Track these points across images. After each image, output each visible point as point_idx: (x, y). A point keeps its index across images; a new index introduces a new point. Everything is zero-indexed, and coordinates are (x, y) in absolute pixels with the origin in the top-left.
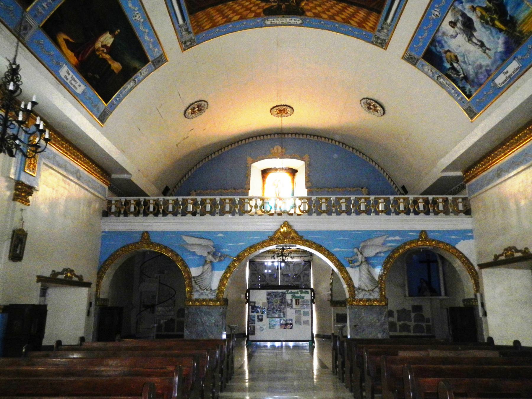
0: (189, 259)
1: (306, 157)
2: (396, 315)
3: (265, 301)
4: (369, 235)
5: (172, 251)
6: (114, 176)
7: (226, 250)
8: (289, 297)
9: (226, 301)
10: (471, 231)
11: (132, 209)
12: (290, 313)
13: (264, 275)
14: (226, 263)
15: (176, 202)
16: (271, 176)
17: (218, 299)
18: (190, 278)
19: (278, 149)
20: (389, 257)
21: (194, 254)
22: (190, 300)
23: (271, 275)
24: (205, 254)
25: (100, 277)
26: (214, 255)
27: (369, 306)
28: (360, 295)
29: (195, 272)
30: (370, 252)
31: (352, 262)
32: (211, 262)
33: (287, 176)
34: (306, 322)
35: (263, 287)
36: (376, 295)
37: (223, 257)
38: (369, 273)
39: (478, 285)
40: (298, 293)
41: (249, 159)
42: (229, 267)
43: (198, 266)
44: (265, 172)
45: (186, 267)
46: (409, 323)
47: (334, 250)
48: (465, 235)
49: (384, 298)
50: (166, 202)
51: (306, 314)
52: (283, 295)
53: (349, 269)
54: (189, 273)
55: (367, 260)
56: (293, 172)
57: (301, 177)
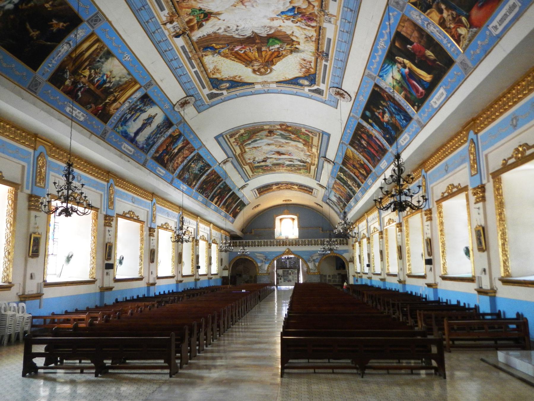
0: (258, 261)
1: (298, 214)
2: (331, 277)
3: (282, 273)
4: (315, 252)
5: (252, 258)
6: (232, 233)
7: (269, 258)
8: (290, 271)
9: (269, 273)
10: (348, 250)
11: (238, 244)
12: (290, 277)
13: (282, 262)
14: (269, 262)
15: (252, 242)
16: (283, 221)
17: (267, 273)
18: (258, 267)
19: (286, 211)
20: (321, 259)
21: (259, 259)
22: (258, 273)
23: (285, 262)
24: (263, 259)
25: (229, 266)
26: (265, 259)
27: (314, 274)
28: (311, 271)
29: (259, 264)
30: (315, 258)
31: (309, 261)
32: (265, 262)
33: (291, 221)
34: (296, 280)
35: (281, 269)
36: (316, 271)
37: (268, 260)
38: (315, 264)
39: (348, 267)
40: (293, 270)
41: (275, 216)
42: (270, 263)
43: (260, 263)
44: (281, 220)
45: (257, 263)
46: (335, 279)
47: (304, 257)
48: (346, 251)
49: (319, 272)
50: (249, 242)
51: (295, 277)
52: (288, 271)
53: (308, 263)
54: (258, 265)
55: (314, 260)
56: (293, 219)
57: (296, 222)
